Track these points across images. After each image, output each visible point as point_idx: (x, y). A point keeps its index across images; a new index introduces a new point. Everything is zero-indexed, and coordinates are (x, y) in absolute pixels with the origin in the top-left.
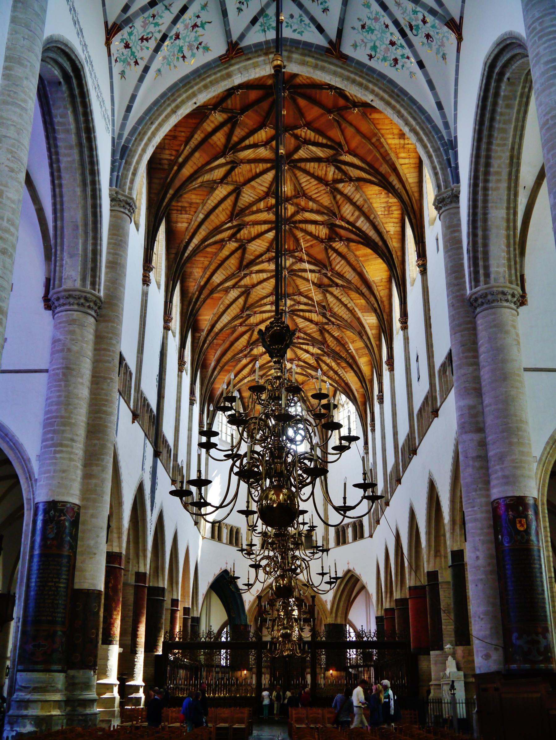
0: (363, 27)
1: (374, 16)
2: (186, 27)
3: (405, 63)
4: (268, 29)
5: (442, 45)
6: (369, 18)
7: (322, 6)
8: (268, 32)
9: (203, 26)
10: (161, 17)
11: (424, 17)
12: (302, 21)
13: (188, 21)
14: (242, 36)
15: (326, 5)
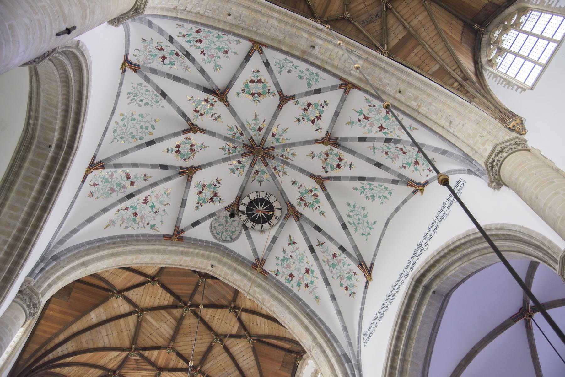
0: (226, 52)
1: (213, 60)
2: (371, 125)
3: (188, 32)
4: (313, 74)
5: (145, 47)
6: (219, 57)
7: (258, 74)
8: (315, 72)
9: (361, 112)
10: (382, 148)
11: (163, 61)
12: (281, 68)
13: (368, 127)
14: (333, 88)
15: (254, 74)
